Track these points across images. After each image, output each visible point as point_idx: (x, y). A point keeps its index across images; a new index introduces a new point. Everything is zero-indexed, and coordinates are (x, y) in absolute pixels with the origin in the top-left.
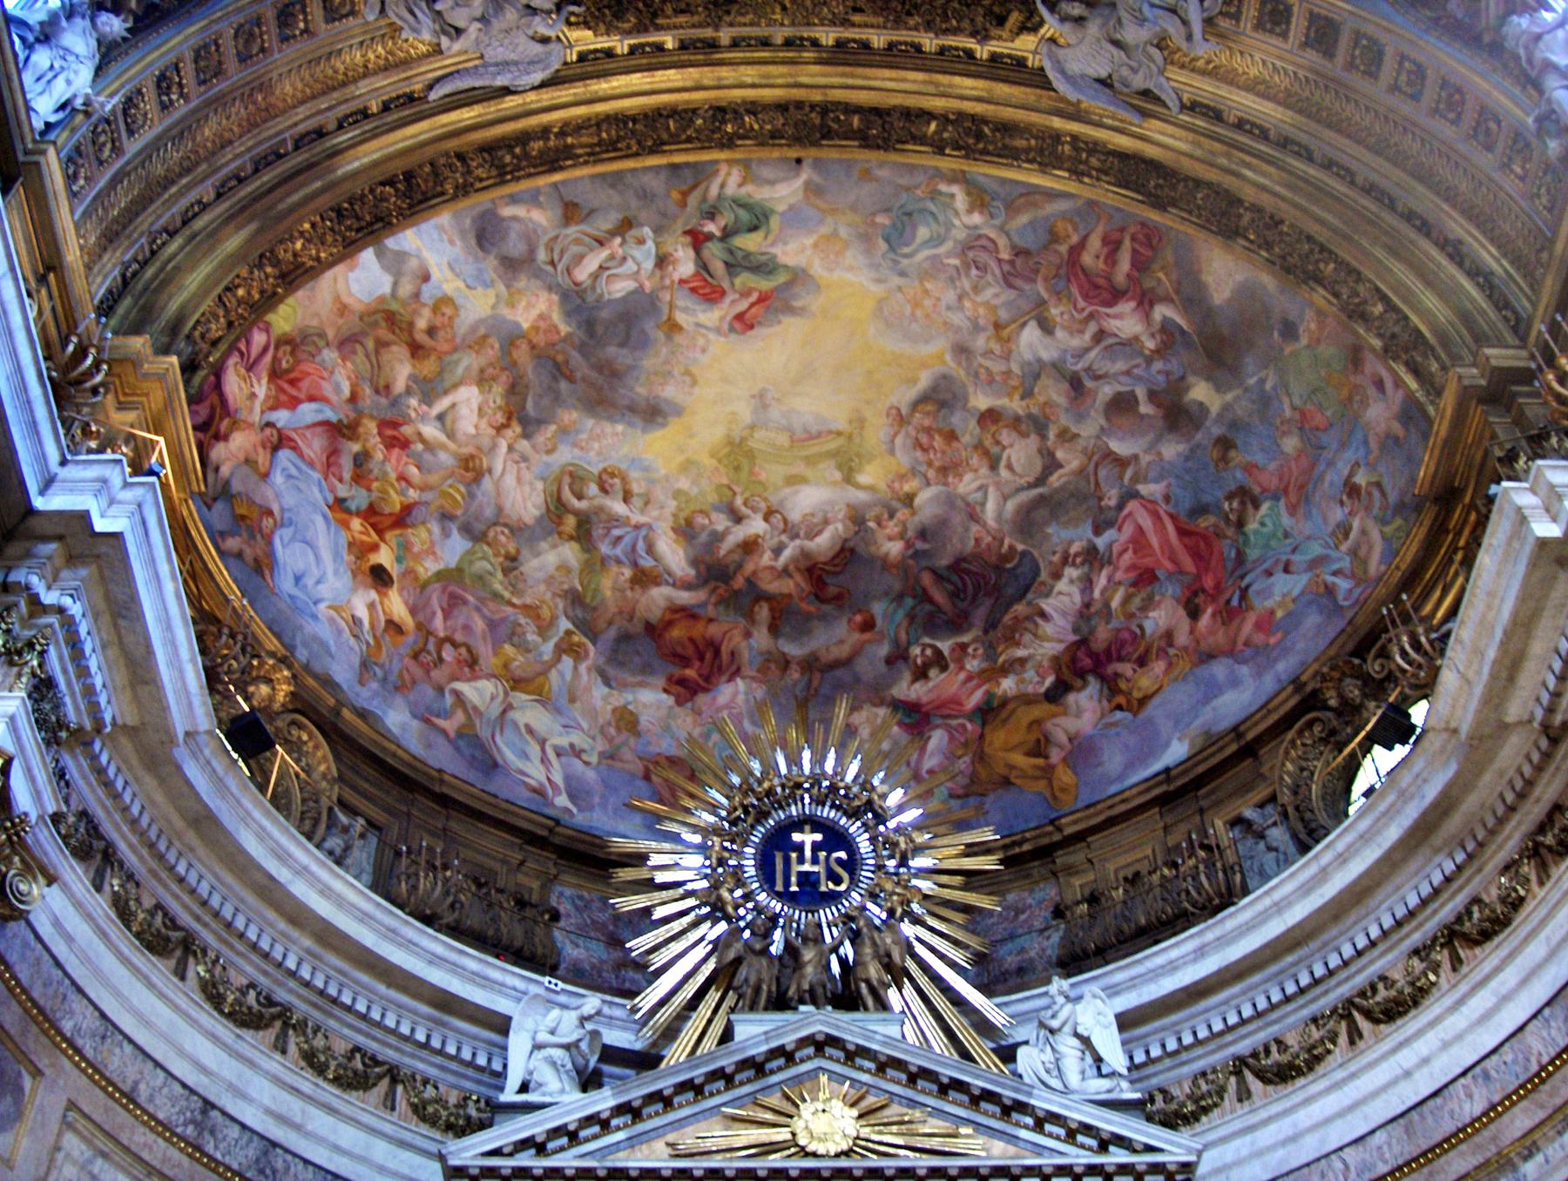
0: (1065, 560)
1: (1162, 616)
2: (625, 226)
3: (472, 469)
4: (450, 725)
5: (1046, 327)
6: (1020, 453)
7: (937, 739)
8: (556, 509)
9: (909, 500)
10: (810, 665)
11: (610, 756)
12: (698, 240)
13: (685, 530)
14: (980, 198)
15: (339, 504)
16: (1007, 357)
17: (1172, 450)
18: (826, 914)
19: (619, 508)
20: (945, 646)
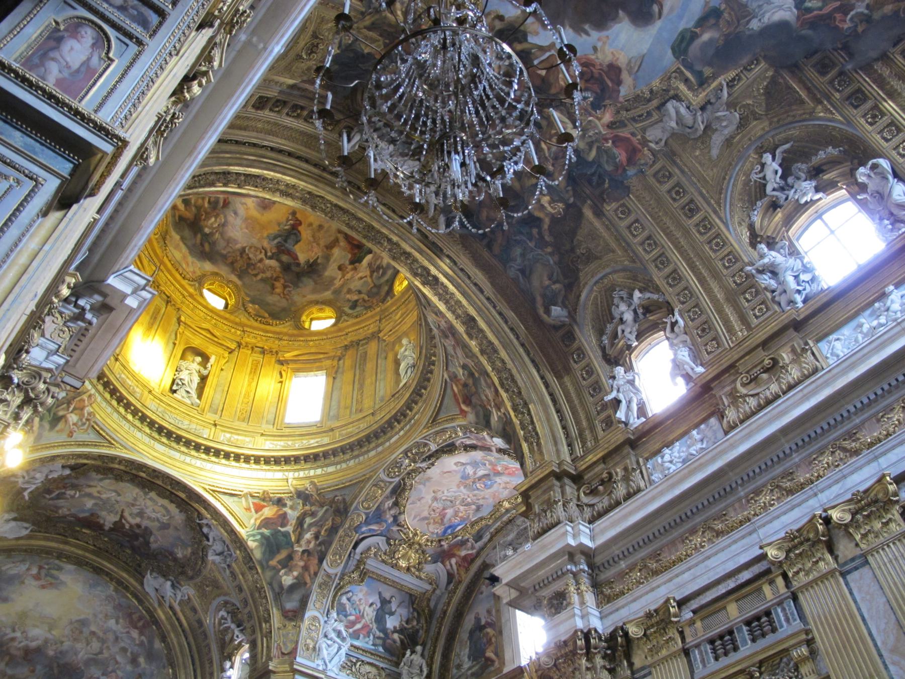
5: (117, 623)
14: (116, 590)
16: (105, 622)
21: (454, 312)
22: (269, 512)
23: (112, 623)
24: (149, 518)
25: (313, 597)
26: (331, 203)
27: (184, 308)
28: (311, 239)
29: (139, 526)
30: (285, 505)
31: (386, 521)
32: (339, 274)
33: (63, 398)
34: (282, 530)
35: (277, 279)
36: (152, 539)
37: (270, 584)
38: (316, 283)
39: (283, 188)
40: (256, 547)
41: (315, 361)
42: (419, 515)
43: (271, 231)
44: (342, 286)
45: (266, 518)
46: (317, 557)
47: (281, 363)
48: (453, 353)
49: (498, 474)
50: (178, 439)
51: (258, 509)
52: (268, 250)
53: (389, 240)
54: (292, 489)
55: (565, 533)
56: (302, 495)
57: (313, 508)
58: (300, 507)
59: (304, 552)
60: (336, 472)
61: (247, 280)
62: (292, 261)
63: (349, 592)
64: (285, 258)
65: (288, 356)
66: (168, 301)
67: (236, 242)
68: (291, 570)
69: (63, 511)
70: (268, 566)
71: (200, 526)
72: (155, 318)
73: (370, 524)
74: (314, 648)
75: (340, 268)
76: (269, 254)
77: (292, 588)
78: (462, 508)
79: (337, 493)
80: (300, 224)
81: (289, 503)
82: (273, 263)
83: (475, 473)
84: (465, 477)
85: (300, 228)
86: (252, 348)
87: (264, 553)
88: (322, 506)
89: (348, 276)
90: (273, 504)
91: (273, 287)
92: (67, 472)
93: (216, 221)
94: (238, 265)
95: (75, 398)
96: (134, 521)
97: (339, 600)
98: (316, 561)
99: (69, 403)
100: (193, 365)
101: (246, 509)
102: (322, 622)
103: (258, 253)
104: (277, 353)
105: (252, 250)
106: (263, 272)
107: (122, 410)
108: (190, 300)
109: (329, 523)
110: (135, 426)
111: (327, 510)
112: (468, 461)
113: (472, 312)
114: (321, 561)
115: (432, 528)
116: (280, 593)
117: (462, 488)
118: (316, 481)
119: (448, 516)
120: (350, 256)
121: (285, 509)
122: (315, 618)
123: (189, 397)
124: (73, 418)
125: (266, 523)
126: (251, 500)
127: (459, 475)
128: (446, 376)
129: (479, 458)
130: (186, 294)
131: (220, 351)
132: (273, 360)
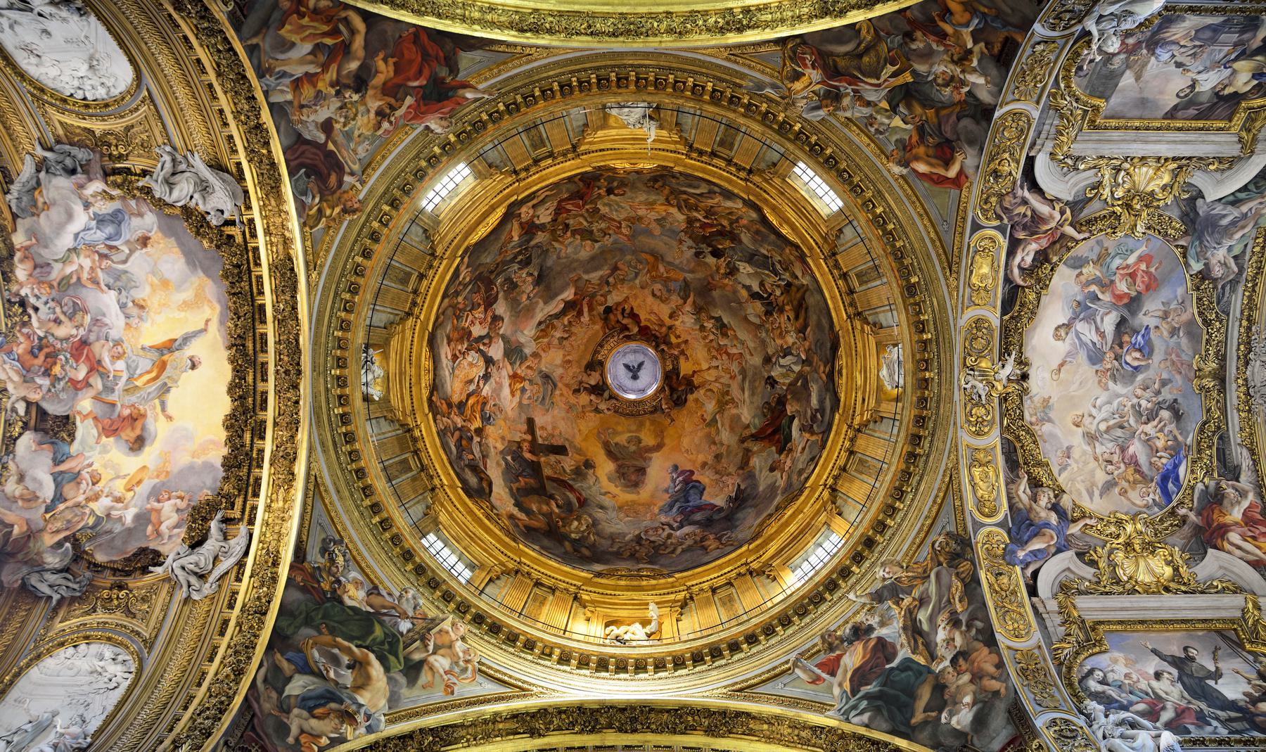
22: (853, 658)
28: (717, 476)
30: (870, 629)
31: (1047, 525)
32: (777, 474)
33: (409, 631)
34: (894, 664)
35: (703, 539)
38: (755, 506)
39: (477, 15)
40: (870, 719)
42: (1093, 484)
43: (661, 504)
44: (789, 477)
45: (856, 671)
46: (978, 645)
47: (760, 572)
48: (866, 111)
49: (1133, 304)
51: (832, 668)
52: (671, 522)
54: (863, 600)
57: (916, 593)
59: (954, 661)
61: (663, 561)
62: (708, 513)
63: (1091, 672)
64: (698, 516)
67: (625, 535)
68: (956, 702)
70: (914, 728)
73: (1026, 543)
75: (772, 469)
76: (675, 525)
77: (980, 721)
78: (1149, 428)
80: (692, 473)
81: (874, 621)
82: (687, 529)
83: (1102, 335)
84: (1095, 357)
85: (694, 478)
87: (892, 718)
89: (789, 463)
90: (851, 643)
91: (705, 548)
93: (580, 523)
94: (643, 552)
95: (430, 629)
97: (1086, 689)
98: (986, 650)
99: (423, 639)
101: (813, 682)
103: (660, 531)
105: (651, 532)
106: (682, 544)
109: (957, 585)
111: (938, 575)
112: (1069, 314)
114: (990, 640)
115: (1134, 496)
117: (1111, 384)
119: (1143, 460)
120: (774, 448)
121: (873, 636)
124: (441, 662)
125: (860, 677)
126: (810, 665)
127: (1082, 356)
128: (897, 170)
129: (1077, 289)
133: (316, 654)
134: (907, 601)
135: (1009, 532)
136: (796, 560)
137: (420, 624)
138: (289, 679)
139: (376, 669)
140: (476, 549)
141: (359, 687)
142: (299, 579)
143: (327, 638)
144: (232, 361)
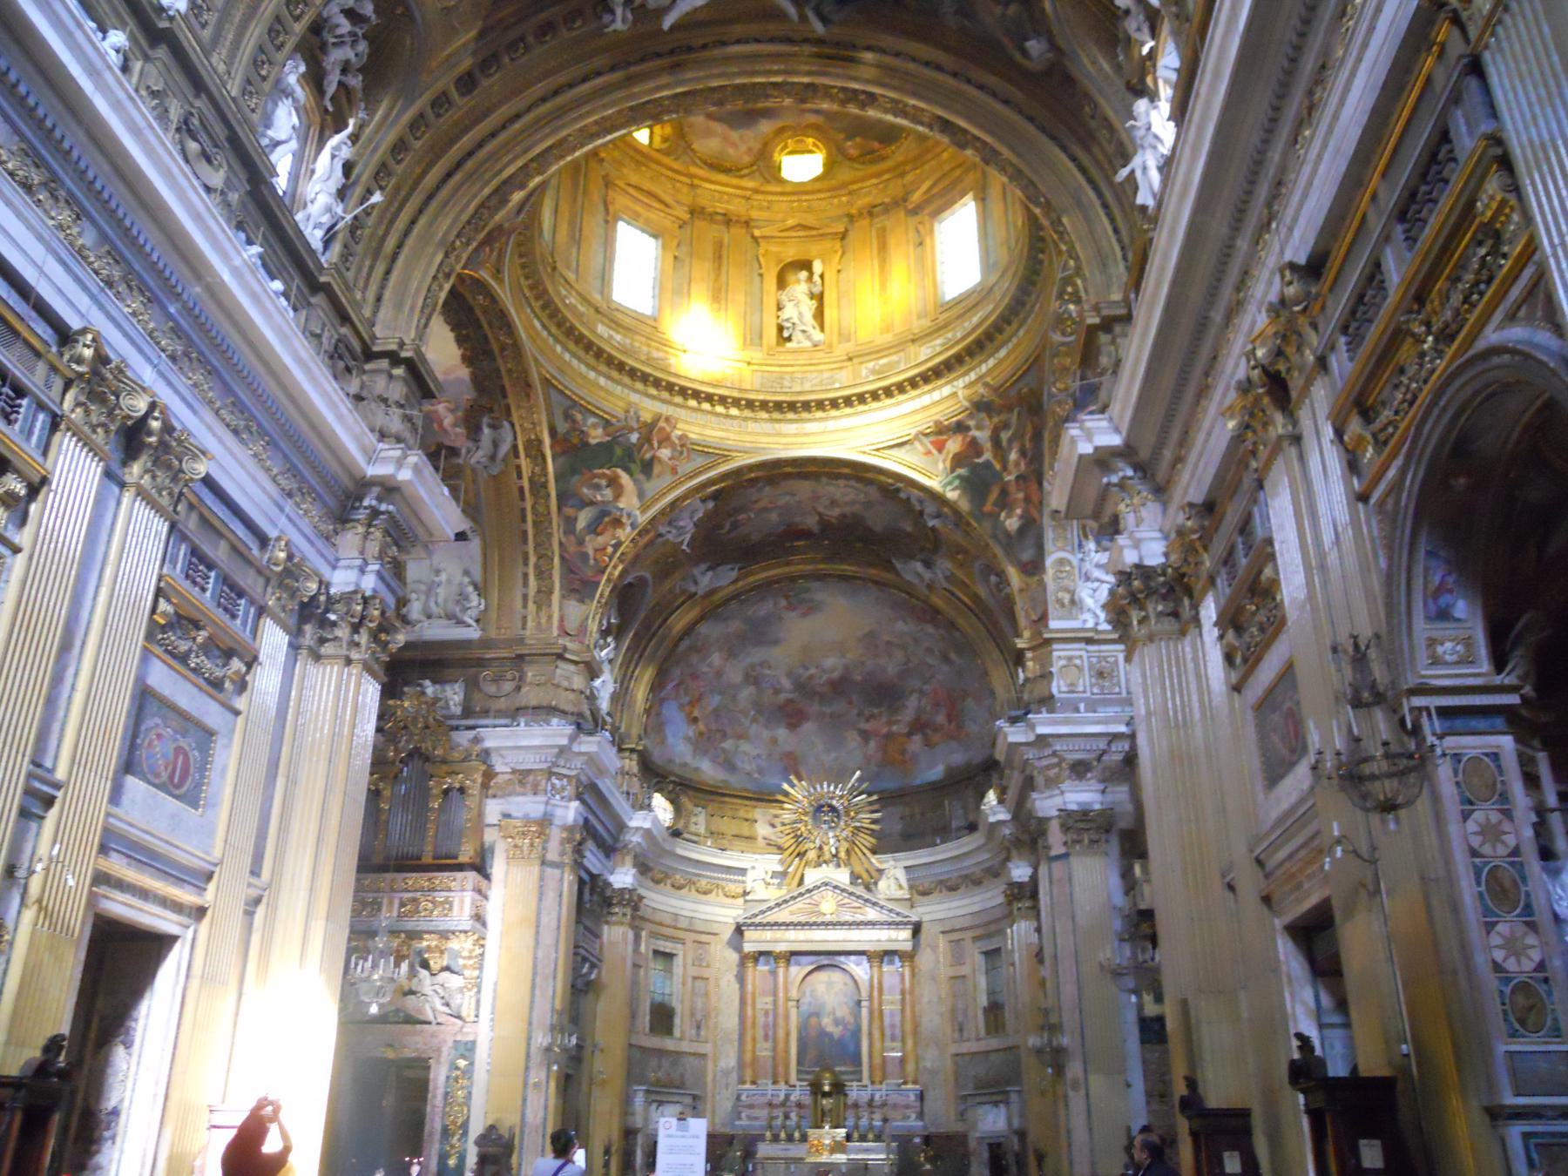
0: (913, 691)
1: (940, 718)
2: (763, 599)
3: (719, 674)
4: (721, 760)
6: (899, 655)
7: (872, 744)
8: (747, 677)
9: (863, 663)
10: (832, 715)
11: (770, 755)
12: (787, 597)
13: (789, 674)
15: (681, 707)
17: (945, 668)
18: (831, 834)
19: (767, 672)
20: (876, 711)
21: (922, 124)
22: (954, 445)
23: (900, 625)
24: (846, 504)
25: (1049, 535)
26: (668, 98)
27: (754, 214)
29: (844, 516)
30: (968, 428)
36: (870, 523)
37: (994, 536)
41: (953, 184)
47: (915, 212)
50: (806, 406)
53: (775, 85)
54: (966, 404)
55: (1073, 441)
56: (981, 406)
58: (987, 422)
59: (1018, 478)
60: (1008, 355)
65: (916, 197)
66: (728, 221)
69: (755, 537)
70: (983, 514)
71: (898, 490)
72: (720, 257)
74: (1073, 602)
77: (1022, 531)
79: (1020, 385)
81: (972, 423)
86: (871, 214)
87: (971, 501)
88: (1010, 409)
92: (711, 505)
96: (836, 512)
98: (1035, 487)
99: (649, 440)
100: (799, 288)
102: (1075, 562)
104: (905, 200)
107: (720, 409)
108: (760, 197)
109: (1029, 428)
110: (745, 419)
113: (940, 112)
114: (1040, 484)
116: (1011, 542)
118: (988, 379)
122: (1061, 562)
123: (809, 338)
124: (665, 453)
125: (958, 461)
126: (926, 441)
130: (748, 193)
131: (827, 244)
132: (902, 214)
133: (585, 490)
134: (996, 420)
135: (1075, 401)
136: (944, 215)
137: (644, 430)
138: (576, 519)
139: (625, 478)
140: (654, 216)
141: (617, 496)
142: (558, 449)
143: (588, 475)
144: (452, 330)
